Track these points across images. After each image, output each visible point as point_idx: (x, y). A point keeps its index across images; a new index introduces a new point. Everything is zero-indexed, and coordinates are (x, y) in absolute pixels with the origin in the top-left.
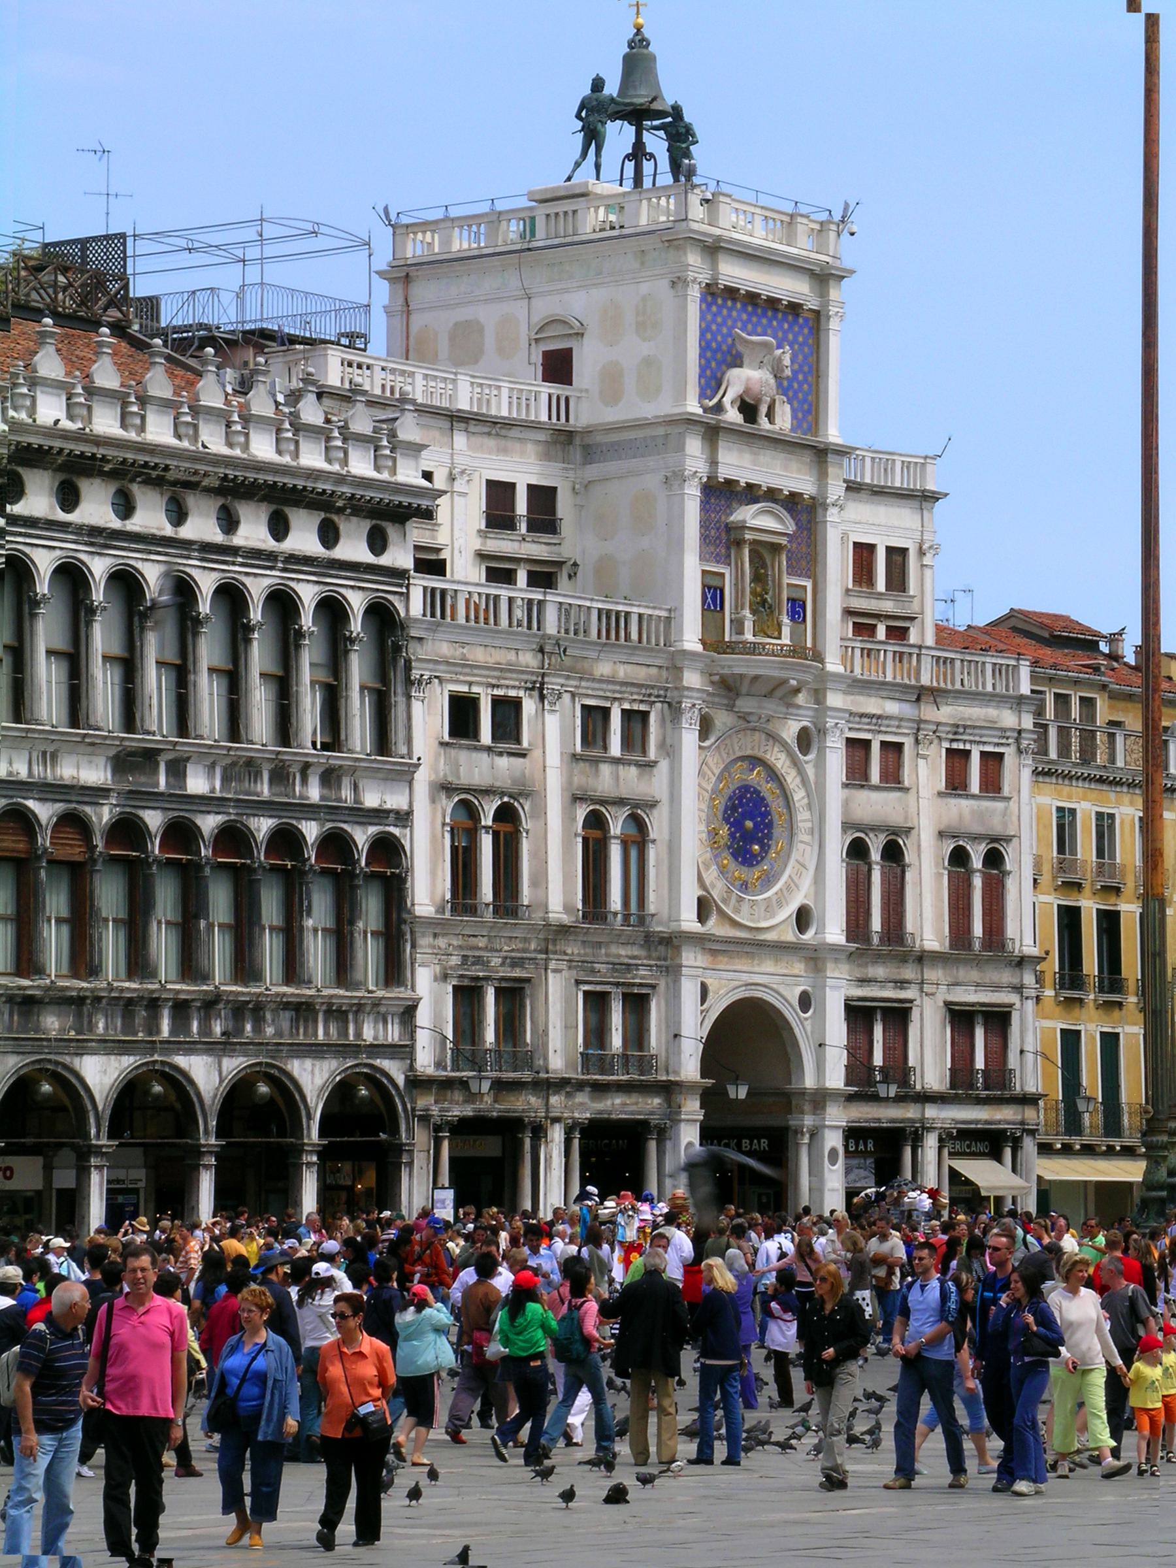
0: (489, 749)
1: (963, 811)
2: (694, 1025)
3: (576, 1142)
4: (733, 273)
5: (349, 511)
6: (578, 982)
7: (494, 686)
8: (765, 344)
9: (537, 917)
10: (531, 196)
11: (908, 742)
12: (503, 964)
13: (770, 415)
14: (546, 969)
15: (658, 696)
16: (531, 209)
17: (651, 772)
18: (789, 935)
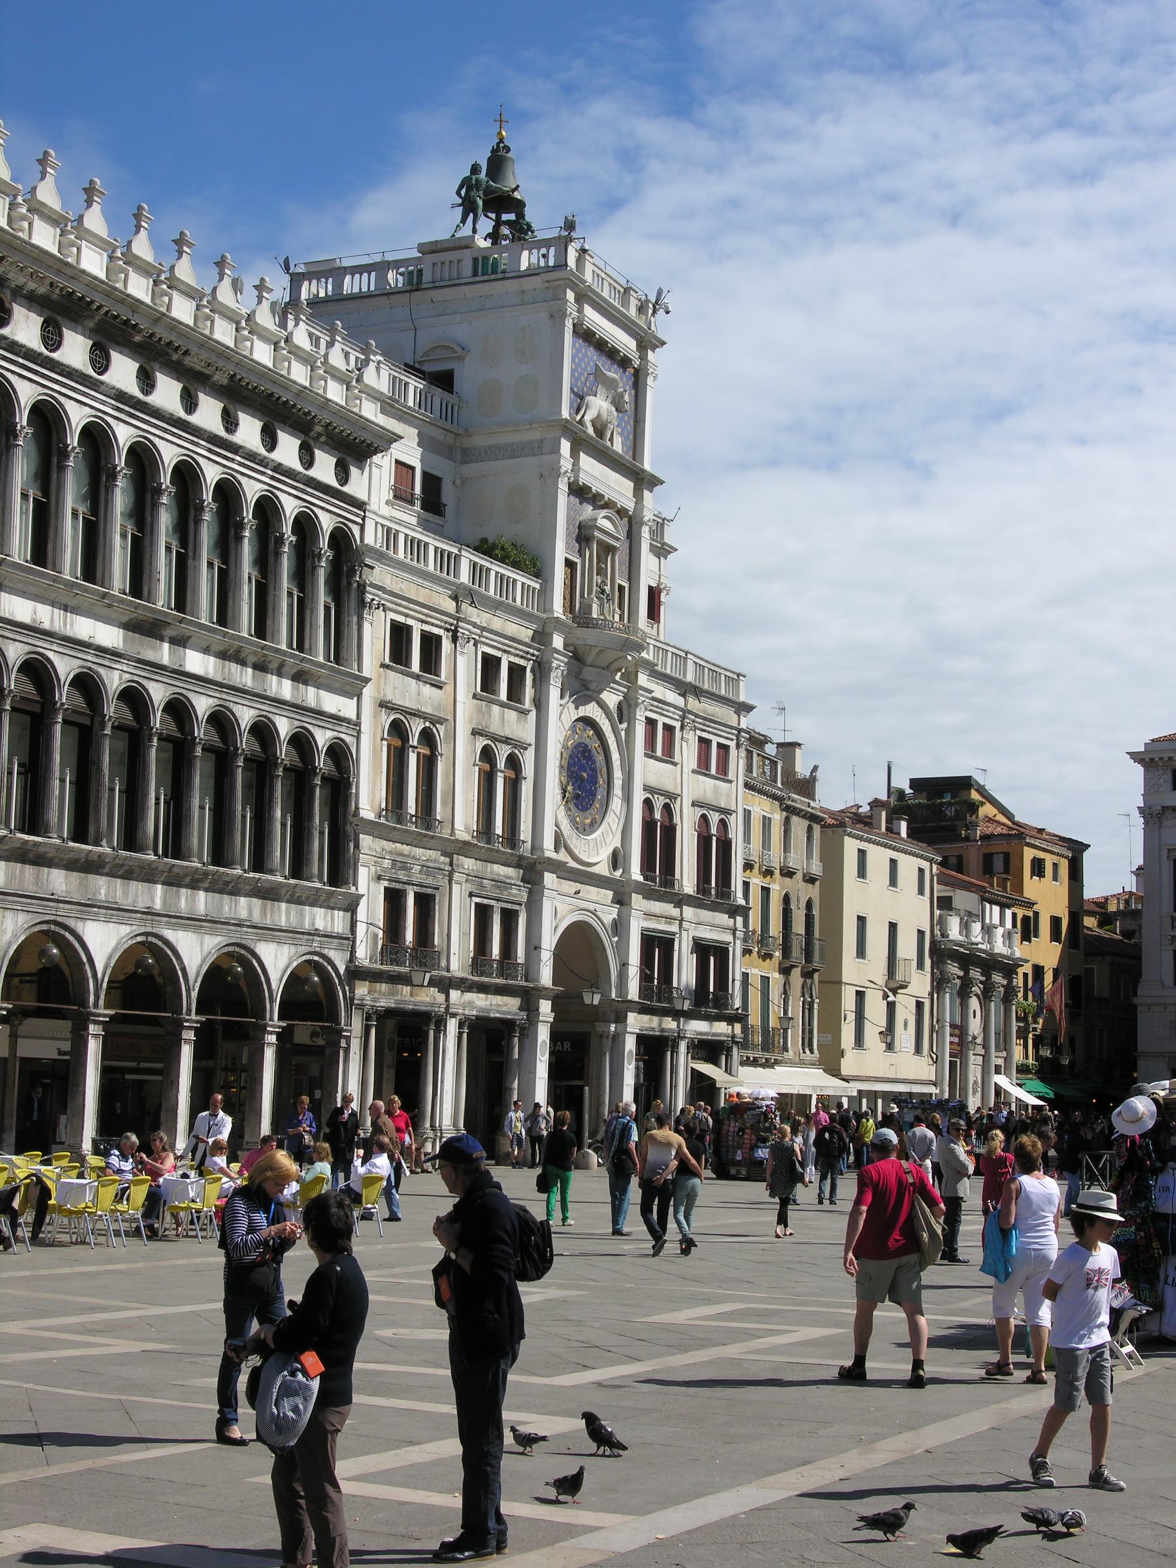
0: (417, 677)
1: (706, 787)
2: (549, 940)
3: (465, 1035)
4: (592, 316)
5: (323, 439)
6: (471, 895)
7: (423, 621)
8: (614, 380)
9: (446, 833)
10: (422, 248)
11: (678, 725)
12: (421, 871)
13: (611, 440)
14: (450, 881)
15: (533, 655)
16: (418, 258)
17: (526, 719)
18: (603, 869)
